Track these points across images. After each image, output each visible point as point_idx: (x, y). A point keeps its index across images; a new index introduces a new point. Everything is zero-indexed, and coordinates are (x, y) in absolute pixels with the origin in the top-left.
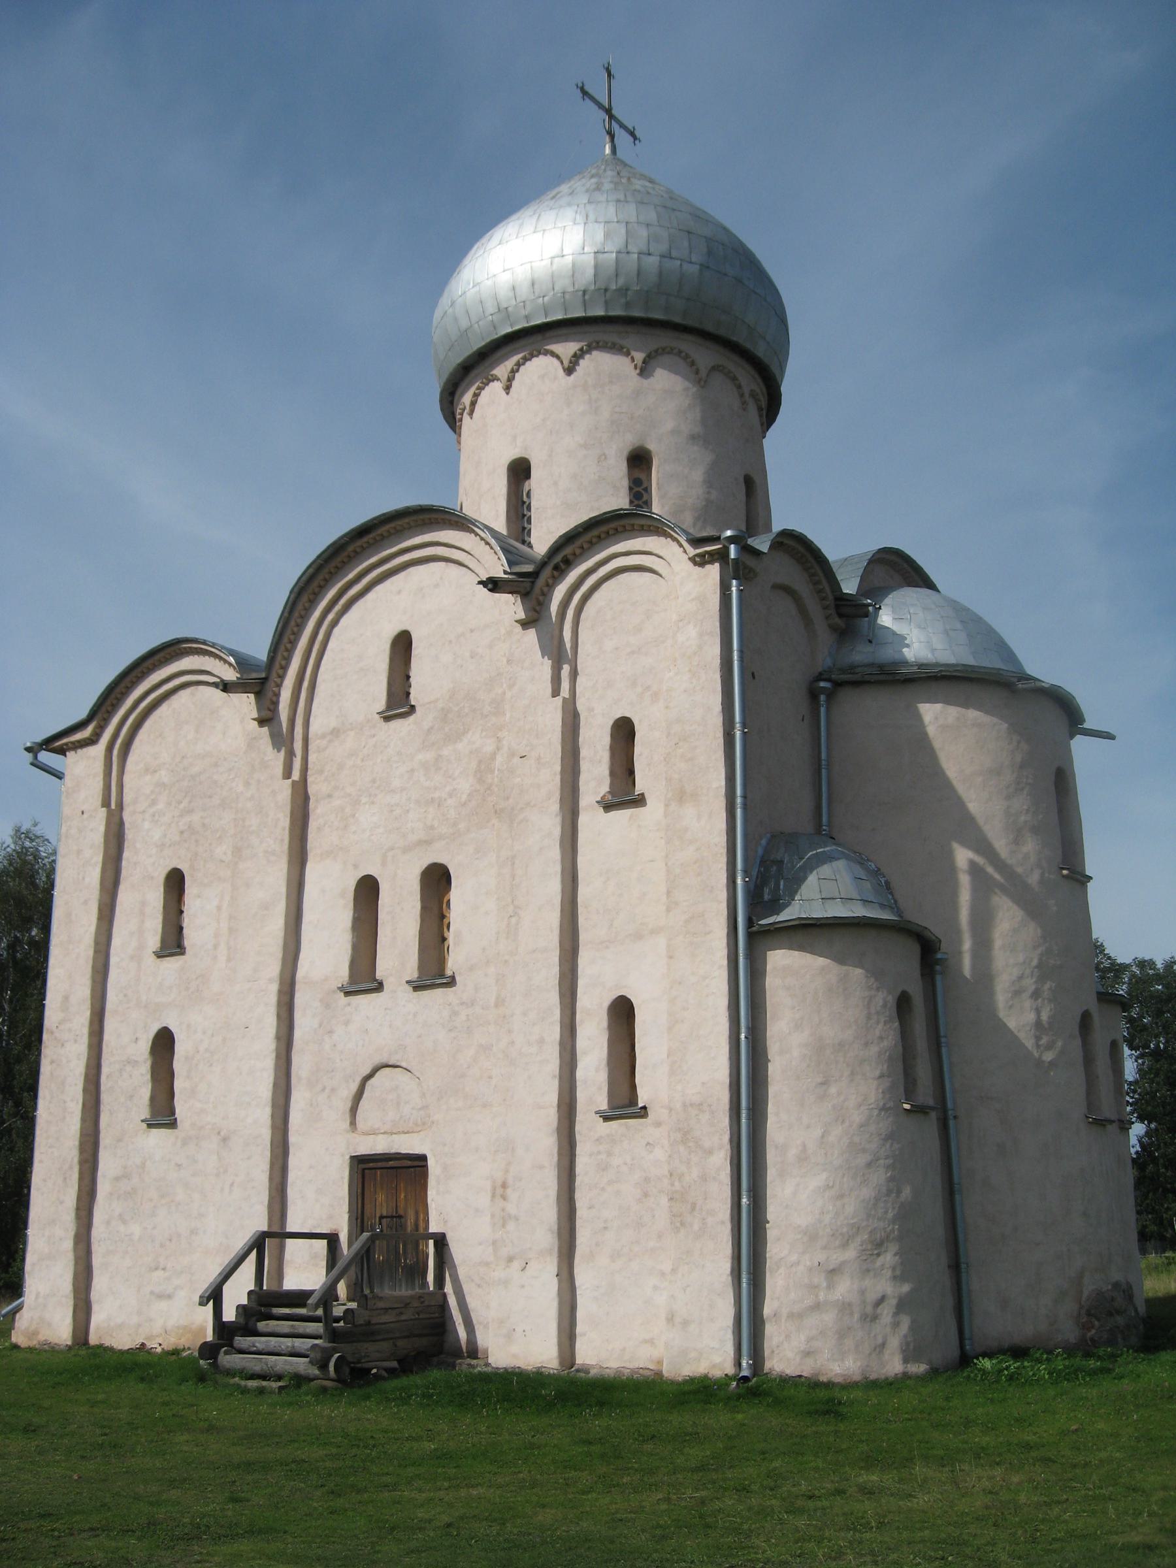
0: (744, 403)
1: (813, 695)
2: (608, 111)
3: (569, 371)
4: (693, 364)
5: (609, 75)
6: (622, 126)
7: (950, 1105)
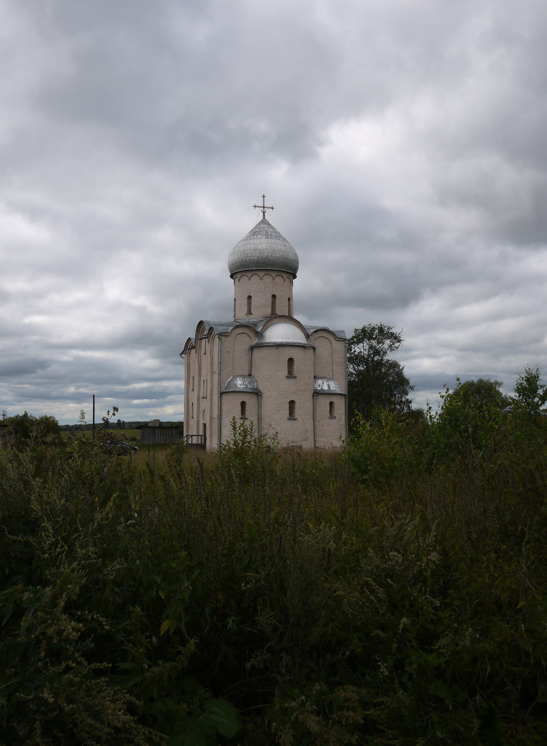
0: (274, 280)
1: (249, 349)
2: (264, 207)
3: (239, 281)
4: (259, 276)
5: (264, 197)
6: (268, 208)
7: (260, 417)
